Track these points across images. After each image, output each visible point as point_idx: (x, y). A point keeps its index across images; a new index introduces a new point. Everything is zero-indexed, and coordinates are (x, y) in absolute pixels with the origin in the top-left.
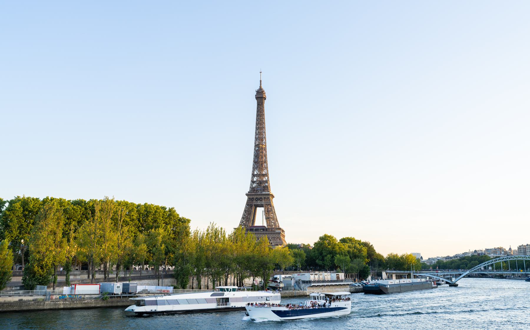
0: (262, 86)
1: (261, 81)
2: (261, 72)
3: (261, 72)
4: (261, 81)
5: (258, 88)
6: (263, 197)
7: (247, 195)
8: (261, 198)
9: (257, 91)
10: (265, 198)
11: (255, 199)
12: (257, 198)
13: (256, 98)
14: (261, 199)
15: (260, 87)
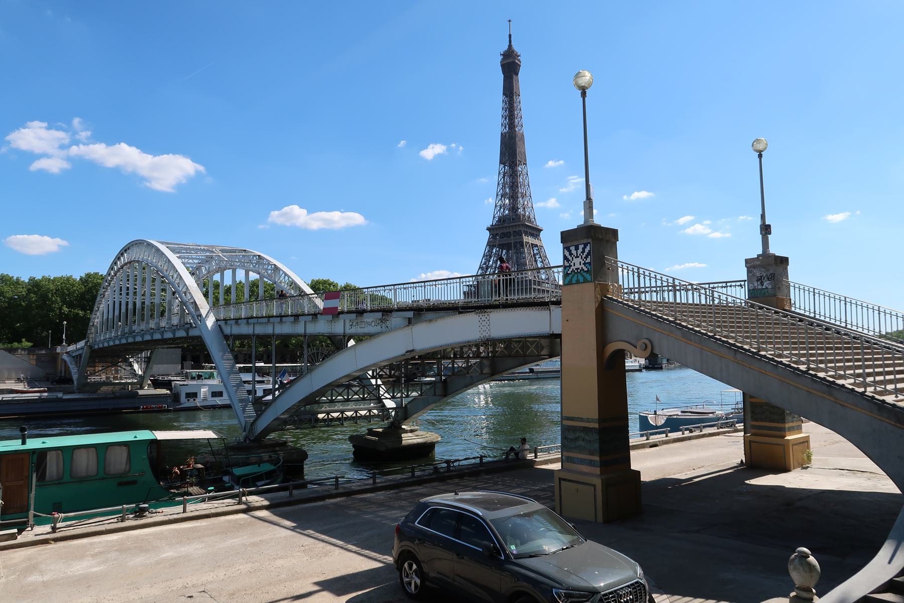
0: (512, 44)
1: (510, 36)
2: (510, 21)
3: (510, 21)
4: (510, 36)
5: (506, 47)
6: (511, 230)
7: (488, 229)
8: (509, 232)
9: (502, 53)
10: (514, 232)
11: (500, 235)
12: (502, 233)
13: (503, 66)
14: (509, 235)
15: (510, 46)
